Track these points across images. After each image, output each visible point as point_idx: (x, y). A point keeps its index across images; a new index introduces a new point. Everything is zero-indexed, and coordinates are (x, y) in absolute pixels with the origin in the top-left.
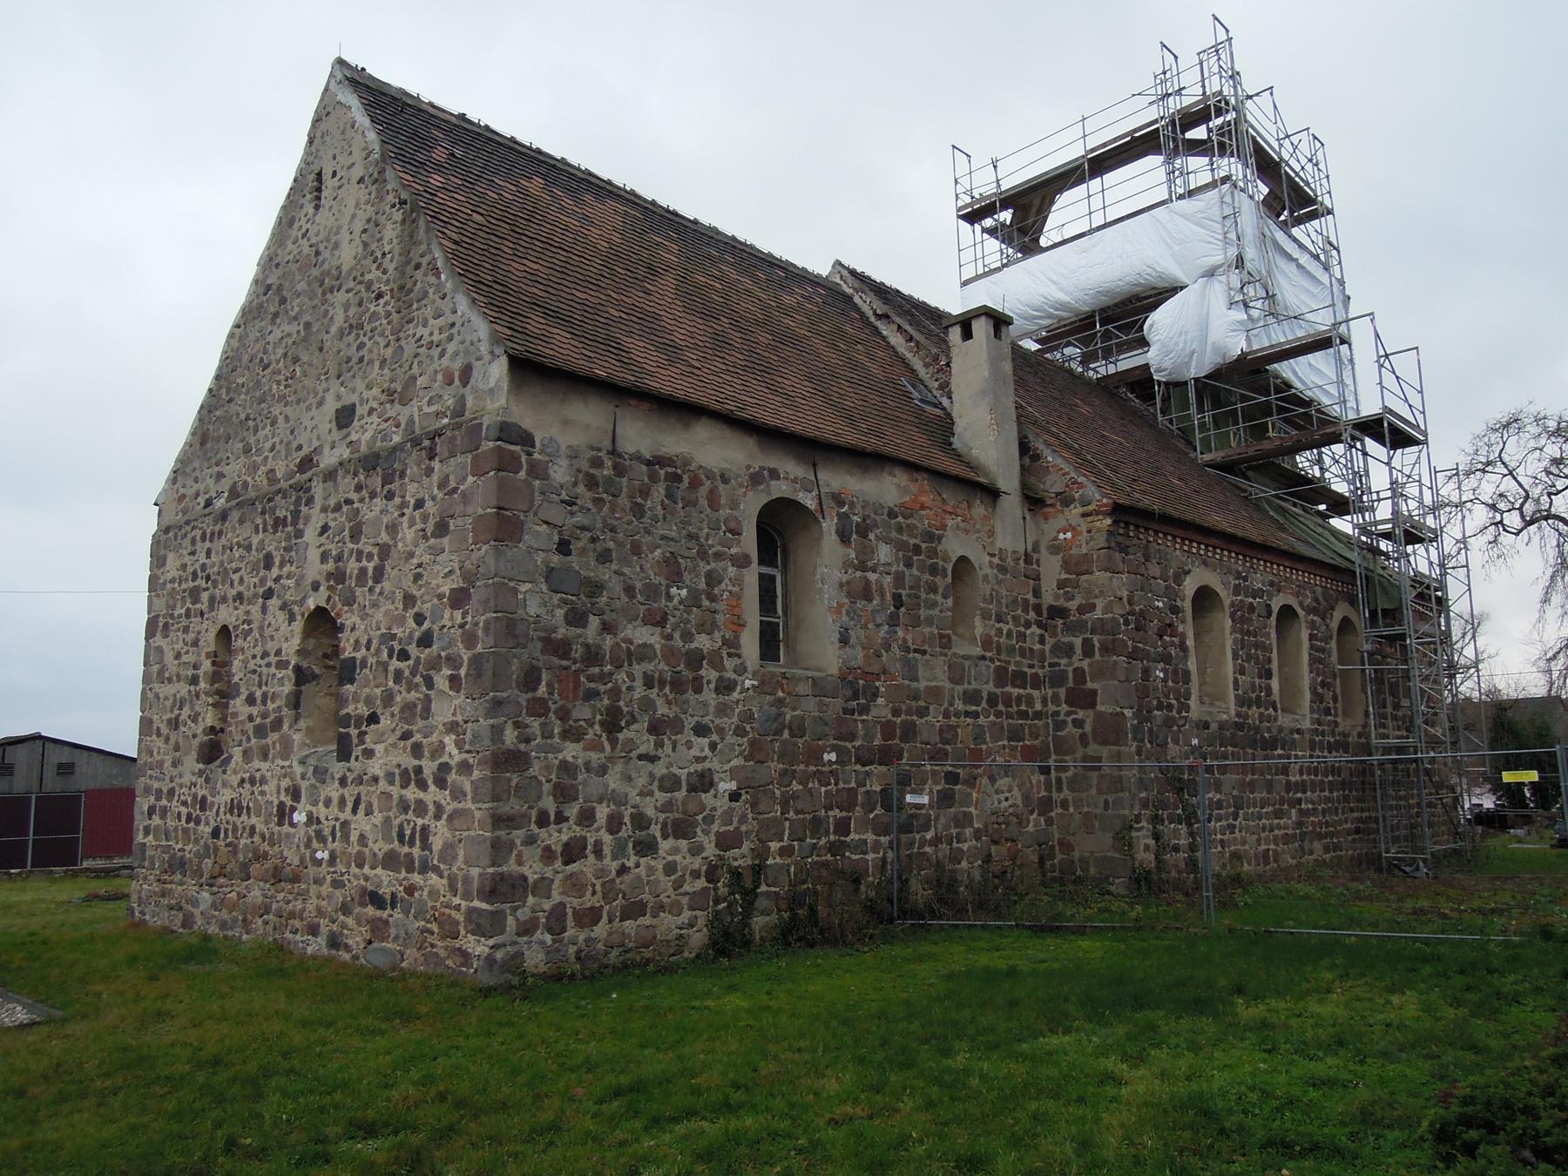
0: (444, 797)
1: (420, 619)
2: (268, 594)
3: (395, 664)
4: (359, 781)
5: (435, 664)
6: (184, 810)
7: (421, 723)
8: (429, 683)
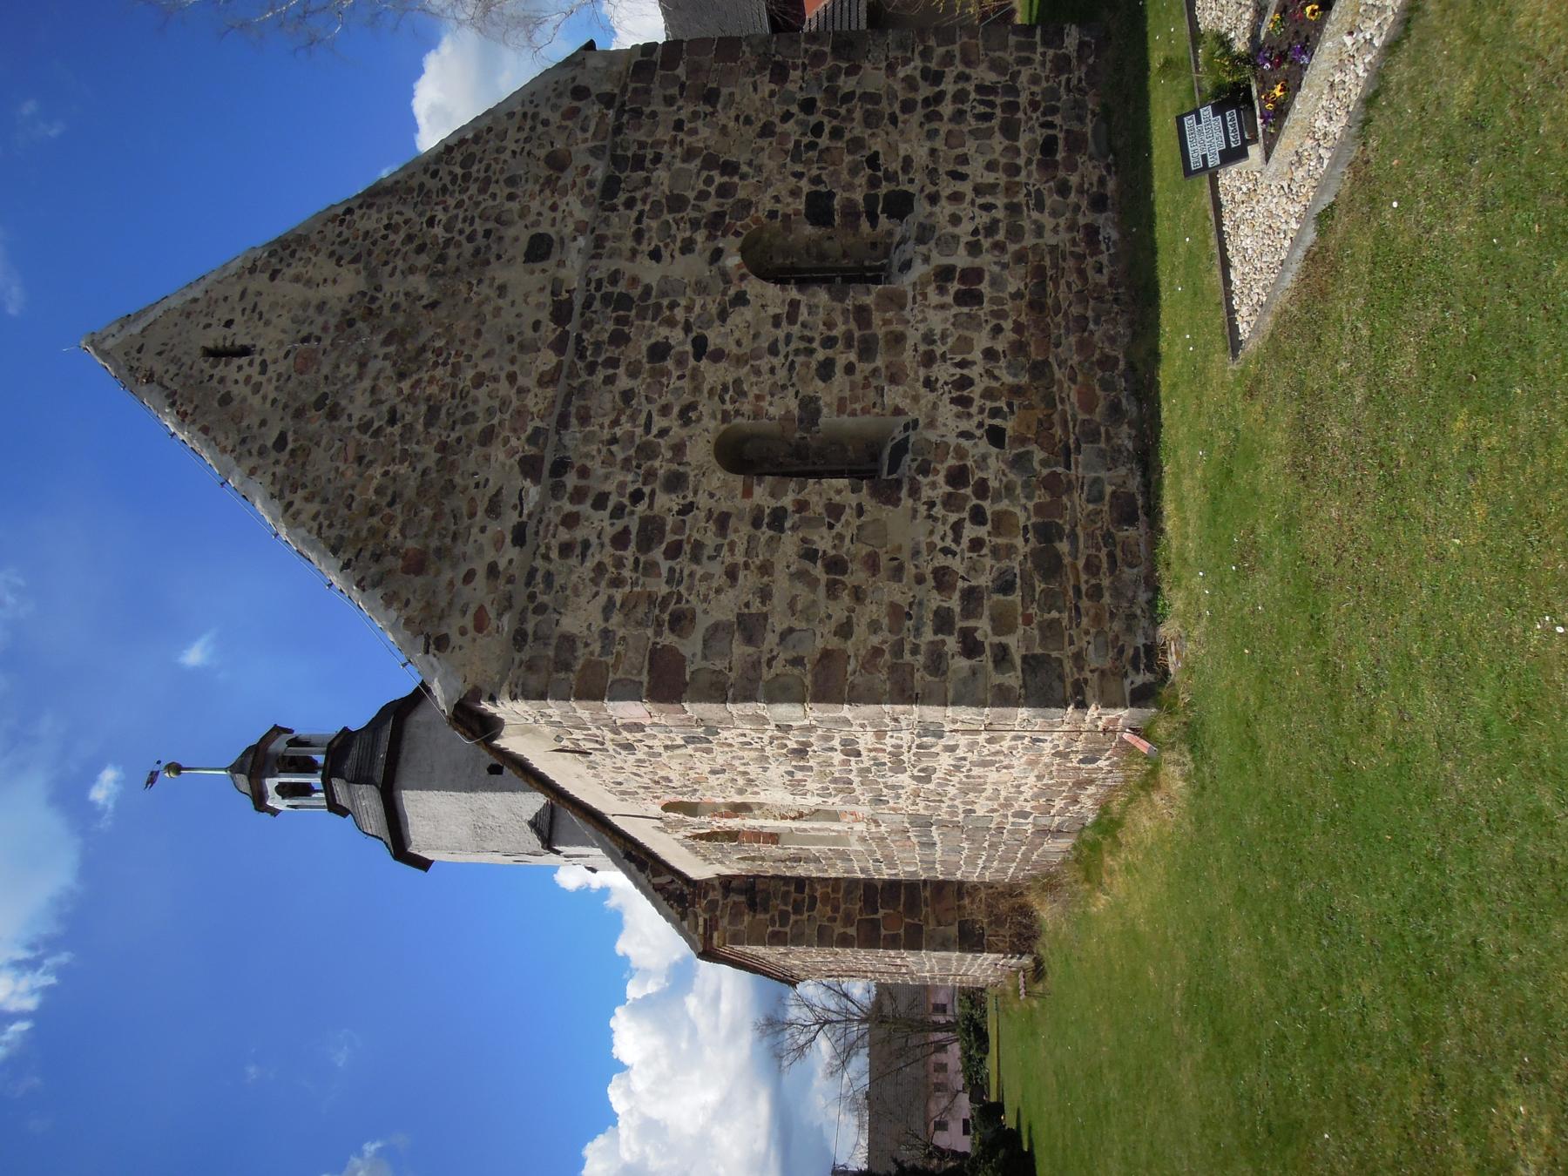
0: (951, 73)
1: (787, 116)
2: (700, 346)
3: (824, 141)
4: (932, 173)
5: (831, 93)
6: (970, 531)
7: (884, 103)
8: (848, 97)
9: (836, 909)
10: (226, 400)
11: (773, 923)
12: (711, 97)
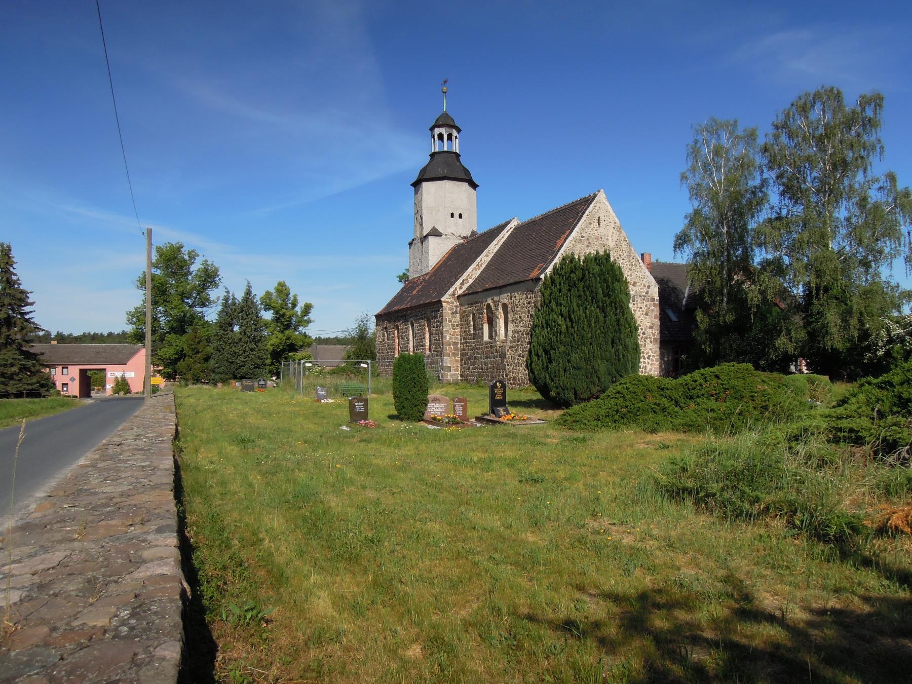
0: (649, 361)
5: (646, 338)
8: (645, 341)
9: (453, 335)
10: (590, 224)
11: (449, 319)
12: (647, 314)
